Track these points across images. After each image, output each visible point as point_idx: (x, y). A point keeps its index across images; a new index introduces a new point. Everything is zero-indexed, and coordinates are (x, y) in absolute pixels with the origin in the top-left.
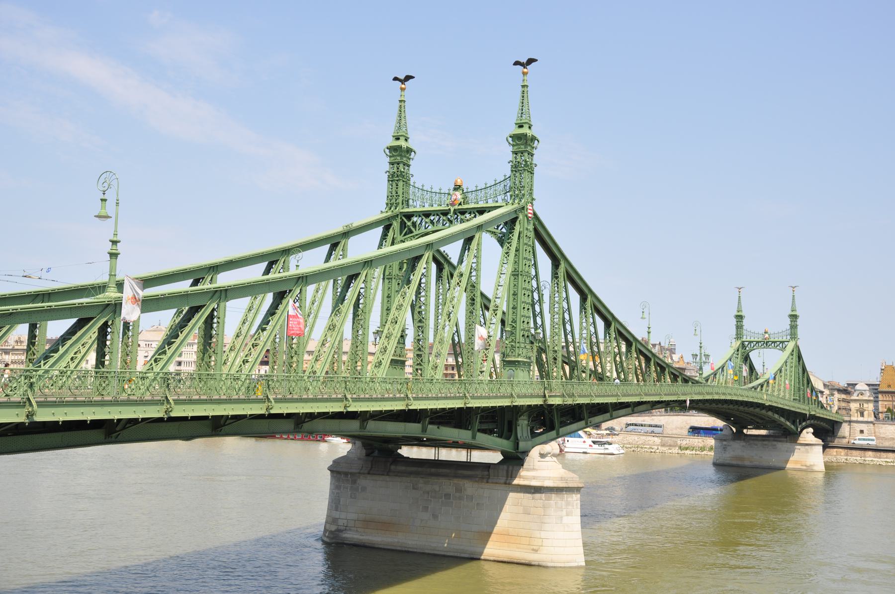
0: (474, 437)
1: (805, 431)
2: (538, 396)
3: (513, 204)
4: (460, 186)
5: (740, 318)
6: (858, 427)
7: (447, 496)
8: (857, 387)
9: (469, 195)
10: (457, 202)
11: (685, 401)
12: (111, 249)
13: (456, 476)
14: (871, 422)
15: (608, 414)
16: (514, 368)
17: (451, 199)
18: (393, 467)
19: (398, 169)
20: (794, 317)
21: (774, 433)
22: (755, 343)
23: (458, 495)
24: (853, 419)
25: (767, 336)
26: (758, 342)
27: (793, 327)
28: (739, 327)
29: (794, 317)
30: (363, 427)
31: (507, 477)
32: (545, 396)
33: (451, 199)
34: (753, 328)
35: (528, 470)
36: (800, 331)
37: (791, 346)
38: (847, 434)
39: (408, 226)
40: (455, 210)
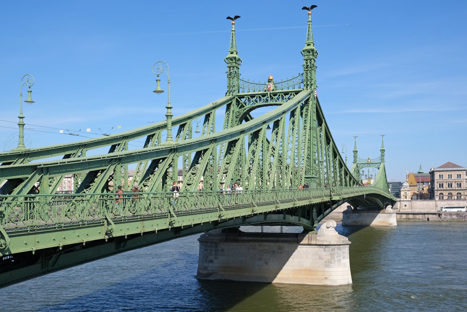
0: (299, 221)
1: (388, 207)
2: (326, 196)
3: (229, 95)
4: (272, 80)
5: (355, 152)
6: (404, 203)
7: (273, 252)
8: (404, 184)
9: (277, 85)
10: (272, 88)
11: (364, 195)
12: (167, 113)
13: (278, 241)
14: (410, 201)
15: (337, 204)
16: (310, 181)
17: (267, 87)
18: (239, 238)
19: (311, 63)
20: (383, 151)
21: (363, 209)
22: (363, 164)
23: (279, 251)
24: (402, 200)
25: (369, 161)
26: (364, 164)
27: (383, 156)
28: (355, 157)
29: (383, 151)
30: (265, 218)
31: (309, 240)
32: (331, 196)
33: (267, 87)
34: (362, 157)
35: (319, 236)
36: (386, 158)
37: (382, 166)
38: (399, 207)
39: (241, 103)
40: (270, 93)
